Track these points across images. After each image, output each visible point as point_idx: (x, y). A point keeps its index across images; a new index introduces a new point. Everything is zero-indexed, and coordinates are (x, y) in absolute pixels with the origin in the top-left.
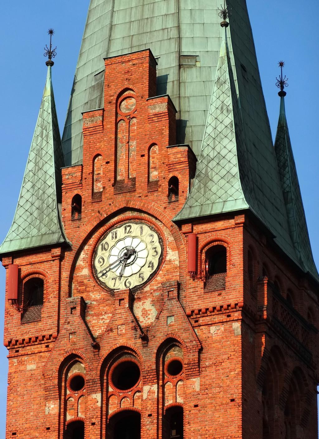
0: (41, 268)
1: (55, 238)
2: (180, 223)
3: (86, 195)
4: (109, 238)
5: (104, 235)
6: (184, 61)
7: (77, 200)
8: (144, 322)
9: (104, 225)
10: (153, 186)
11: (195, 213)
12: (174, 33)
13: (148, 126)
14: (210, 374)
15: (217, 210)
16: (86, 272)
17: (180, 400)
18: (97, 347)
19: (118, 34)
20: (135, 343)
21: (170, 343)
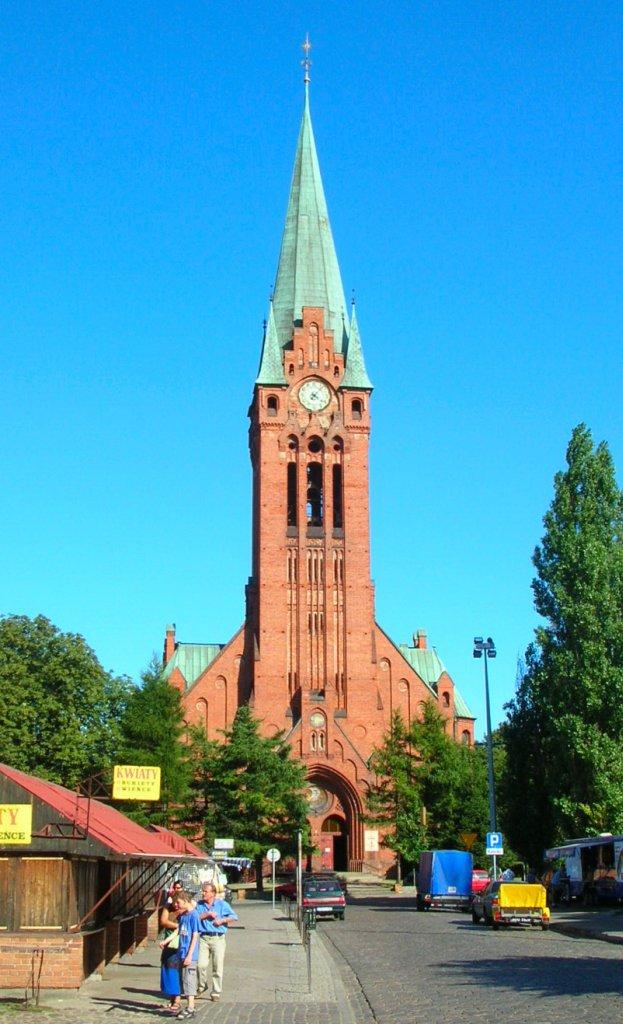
0: (276, 393)
1: (283, 382)
2: (341, 388)
3: (296, 367)
4: (305, 385)
5: (303, 384)
6: (331, 314)
7: (292, 366)
8: (324, 426)
9: (305, 379)
10: (327, 368)
11: (350, 385)
12: (325, 300)
13: (324, 341)
14: (355, 453)
15: (359, 385)
16: (295, 398)
17: (339, 462)
18: (303, 434)
19: (299, 293)
20: (321, 435)
21: (337, 438)
